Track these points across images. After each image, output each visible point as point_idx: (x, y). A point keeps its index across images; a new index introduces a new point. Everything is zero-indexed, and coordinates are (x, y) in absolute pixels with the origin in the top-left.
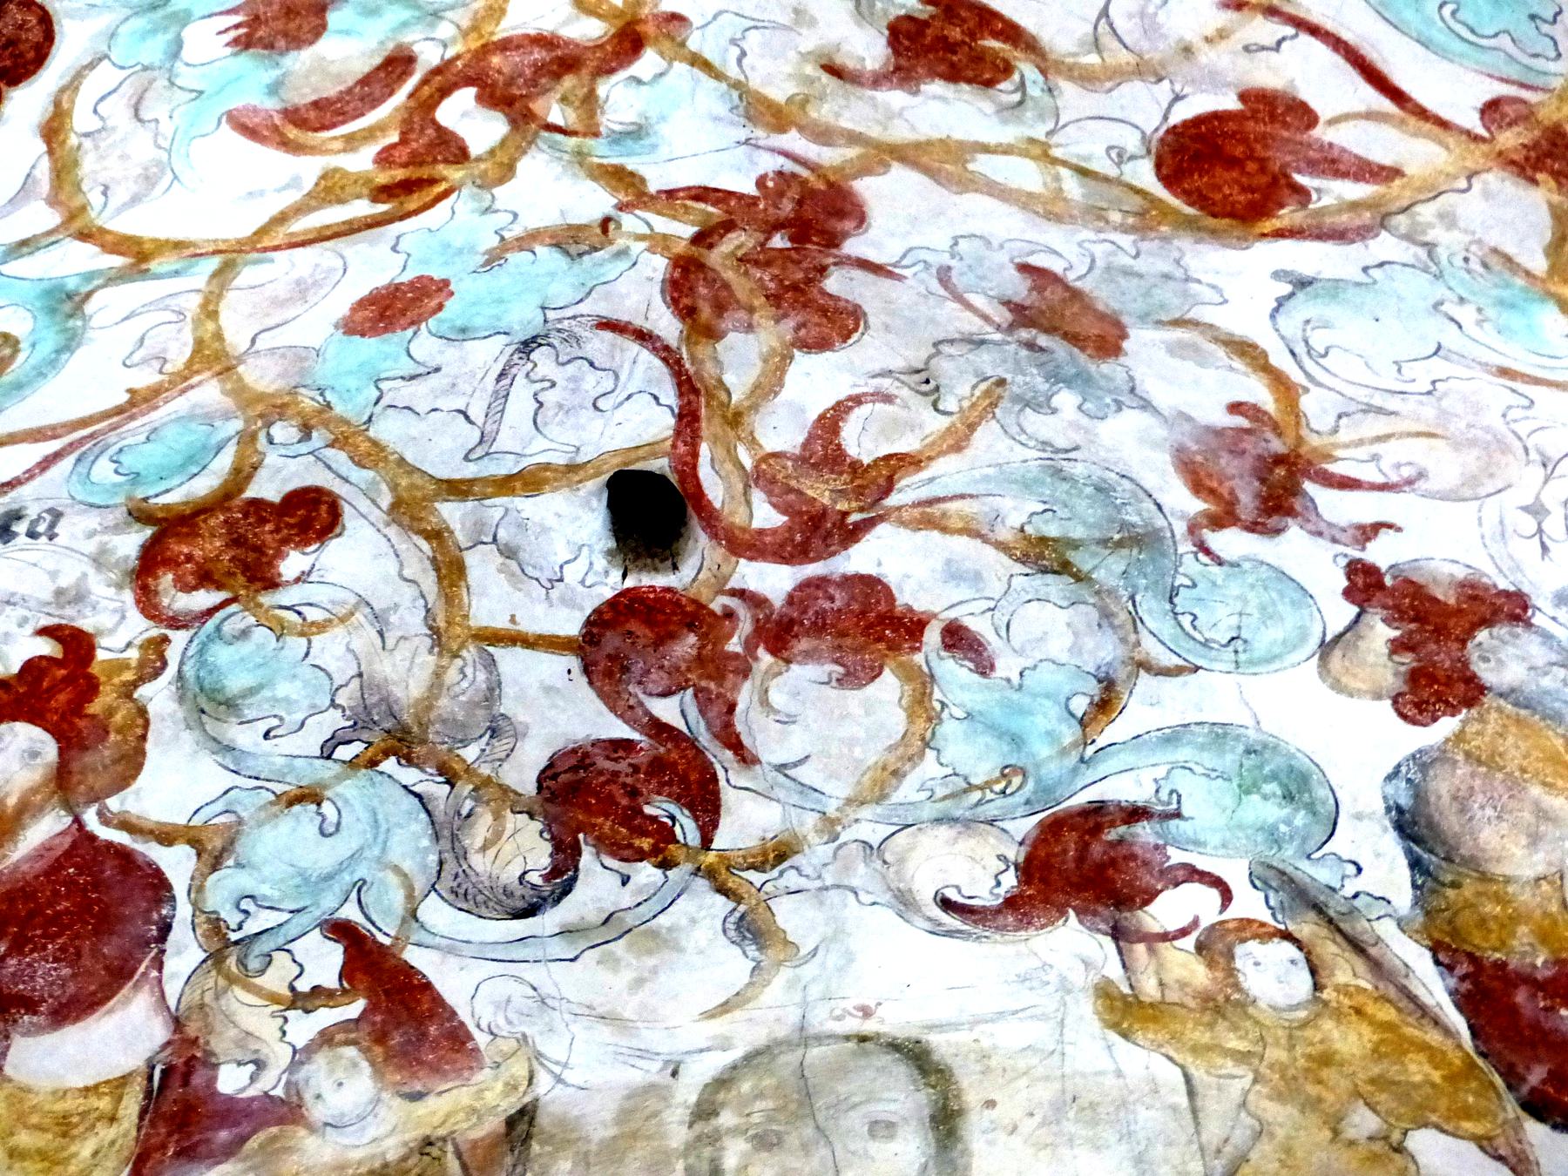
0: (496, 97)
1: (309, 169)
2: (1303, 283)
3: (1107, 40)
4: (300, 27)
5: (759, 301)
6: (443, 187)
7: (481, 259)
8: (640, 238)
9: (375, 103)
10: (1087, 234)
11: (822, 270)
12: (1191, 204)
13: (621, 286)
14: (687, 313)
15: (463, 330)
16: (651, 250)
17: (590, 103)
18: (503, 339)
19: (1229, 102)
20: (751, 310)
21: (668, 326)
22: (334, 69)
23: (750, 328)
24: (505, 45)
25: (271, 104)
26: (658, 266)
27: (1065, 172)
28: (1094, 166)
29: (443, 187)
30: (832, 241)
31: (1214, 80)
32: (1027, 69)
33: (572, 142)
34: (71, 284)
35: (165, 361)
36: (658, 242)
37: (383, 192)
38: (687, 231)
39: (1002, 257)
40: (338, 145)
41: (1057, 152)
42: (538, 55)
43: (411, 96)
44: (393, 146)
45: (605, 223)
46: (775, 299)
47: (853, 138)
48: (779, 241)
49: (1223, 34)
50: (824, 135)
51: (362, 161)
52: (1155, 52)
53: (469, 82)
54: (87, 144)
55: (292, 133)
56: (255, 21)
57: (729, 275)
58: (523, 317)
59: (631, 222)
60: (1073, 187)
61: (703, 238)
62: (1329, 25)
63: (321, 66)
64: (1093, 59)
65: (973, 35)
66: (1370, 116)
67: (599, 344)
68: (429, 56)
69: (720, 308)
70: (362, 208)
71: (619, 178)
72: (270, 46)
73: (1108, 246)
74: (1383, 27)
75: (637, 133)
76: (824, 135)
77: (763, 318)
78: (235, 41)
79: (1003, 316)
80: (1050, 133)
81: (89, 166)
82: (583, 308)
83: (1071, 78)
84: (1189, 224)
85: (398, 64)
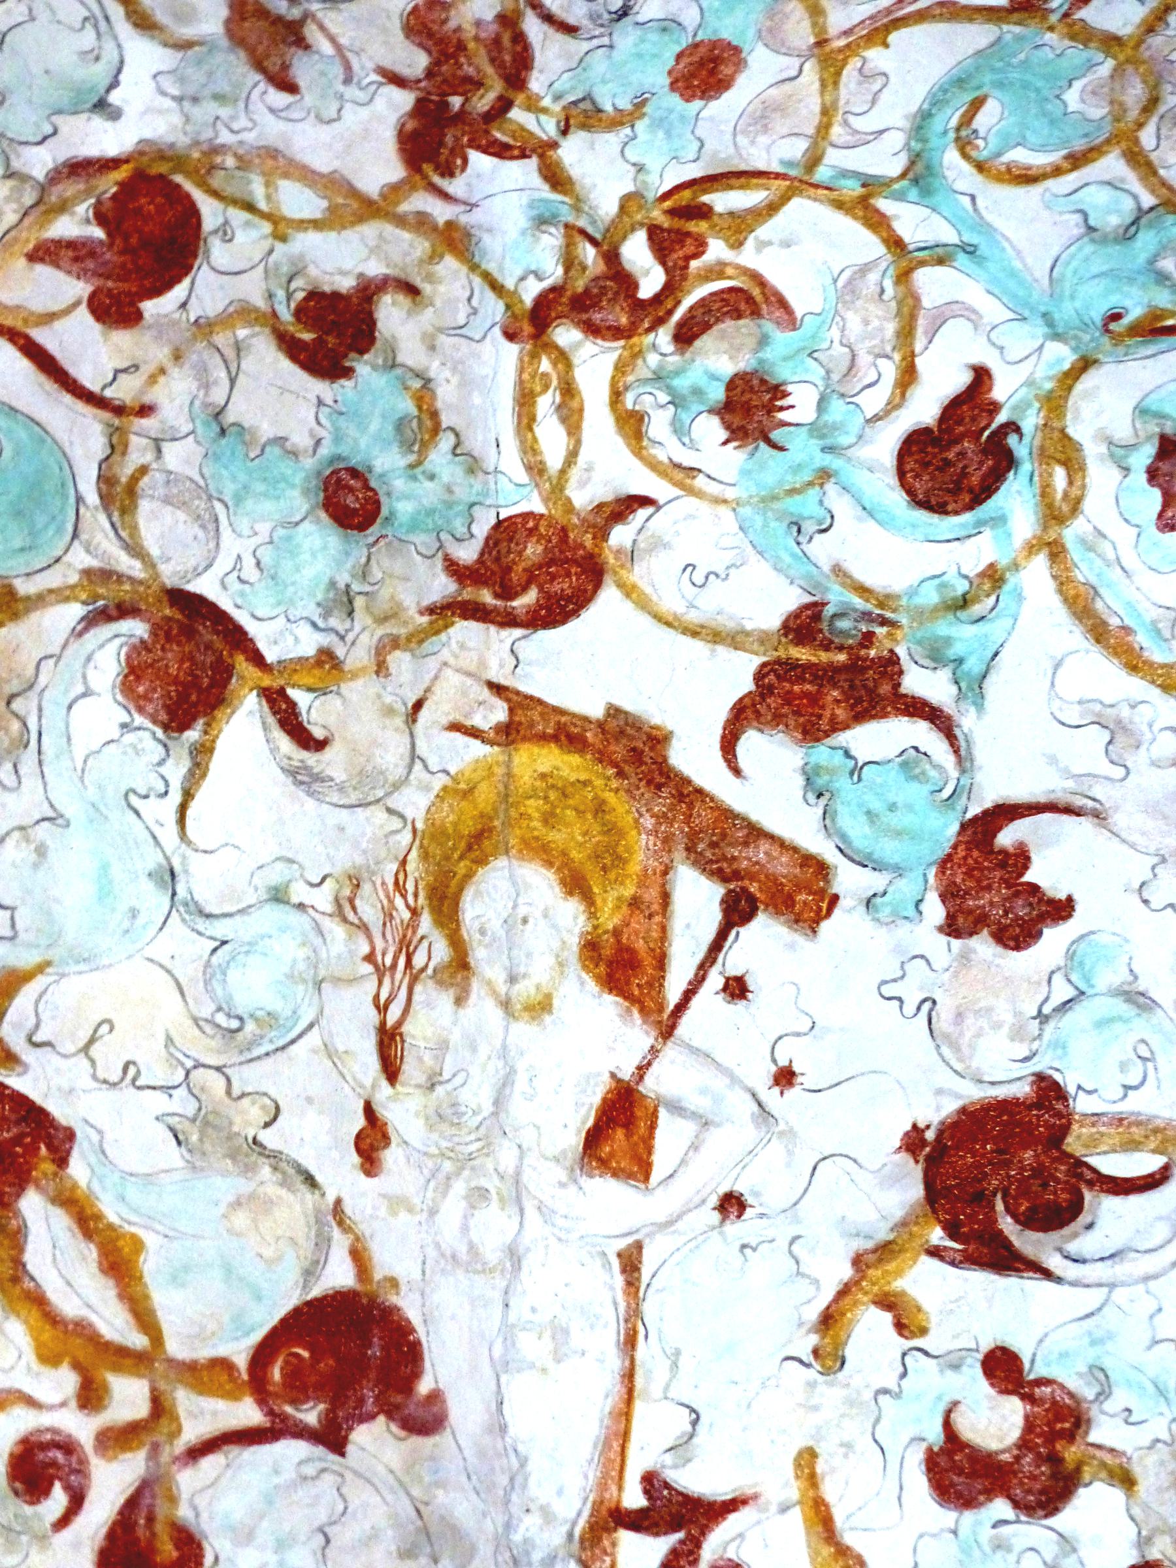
0: (625, 281)
1: (748, 257)
2: (101, 106)
3: (230, 353)
4: (743, 393)
5: (471, 45)
6: (668, 204)
7: (647, 109)
8: (545, 111)
9: (702, 303)
10: (250, 137)
11: (430, 73)
12: (178, 186)
13: (559, 65)
14: (520, 38)
15: (664, 30)
16: (539, 98)
17: (570, 261)
18: (641, 18)
19: (149, 307)
20: (476, 38)
21: (533, 27)
22: (725, 346)
23: (478, 23)
24: (617, 333)
25: (768, 326)
26: (536, 83)
27: (263, 205)
28: (245, 216)
29: (668, 204)
30: (420, 108)
31: (163, 326)
32: (286, 314)
33: (582, 223)
34: (913, 194)
35: (860, 70)
36: (533, 106)
37: (705, 212)
38: (516, 114)
39: (309, 98)
40: (730, 271)
41: (267, 228)
42: (597, 317)
43: (678, 303)
44: (697, 255)
45: (565, 132)
46: (461, 47)
47: (401, 221)
48: (456, 101)
49: (152, 379)
50: (421, 223)
51: (717, 250)
52: (199, 352)
53: (642, 304)
54: (888, 348)
55: (756, 292)
56: (771, 409)
57: (489, 70)
58: (626, 38)
59: (548, 127)
60: (258, 191)
61: (504, 105)
62: (80, 406)
63: (734, 352)
64: (242, 333)
65: (319, 341)
66: (50, 318)
67: (577, 14)
68: (663, 337)
69: (497, 41)
70: (722, 201)
71: (556, 178)
72: (763, 382)
73: (235, 127)
74: (42, 415)
75: (542, 222)
76: (421, 223)
77: (469, 31)
78: (785, 395)
79: (311, 32)
80: (271, 251)
81: (890, 328)
82: (586, 46)
83: (256, 310)
84: (179, 161)
85: (685, 337)
